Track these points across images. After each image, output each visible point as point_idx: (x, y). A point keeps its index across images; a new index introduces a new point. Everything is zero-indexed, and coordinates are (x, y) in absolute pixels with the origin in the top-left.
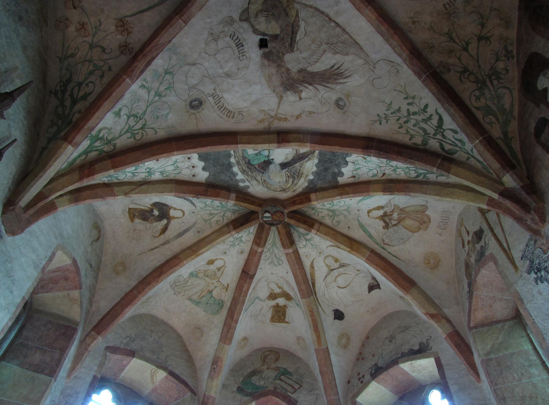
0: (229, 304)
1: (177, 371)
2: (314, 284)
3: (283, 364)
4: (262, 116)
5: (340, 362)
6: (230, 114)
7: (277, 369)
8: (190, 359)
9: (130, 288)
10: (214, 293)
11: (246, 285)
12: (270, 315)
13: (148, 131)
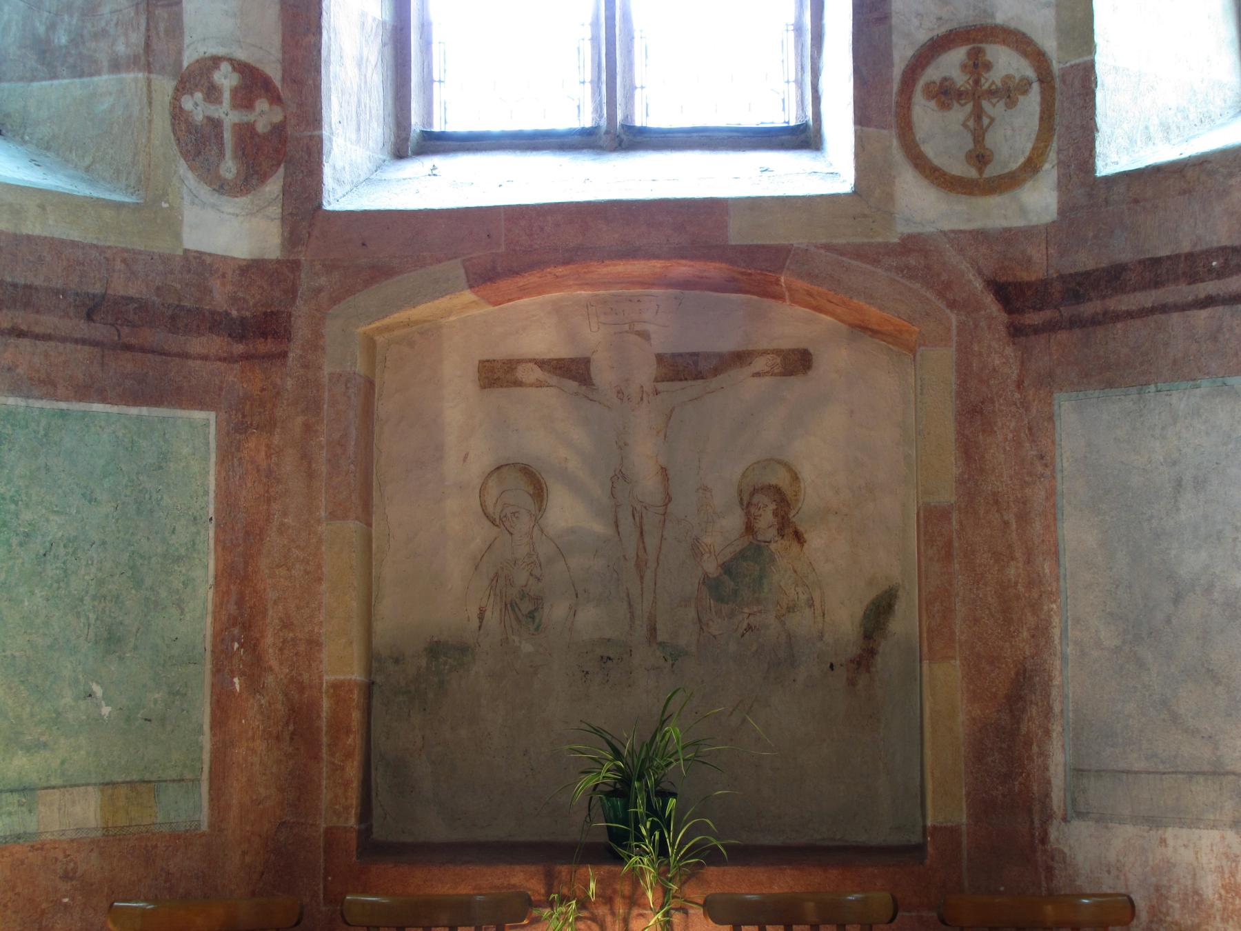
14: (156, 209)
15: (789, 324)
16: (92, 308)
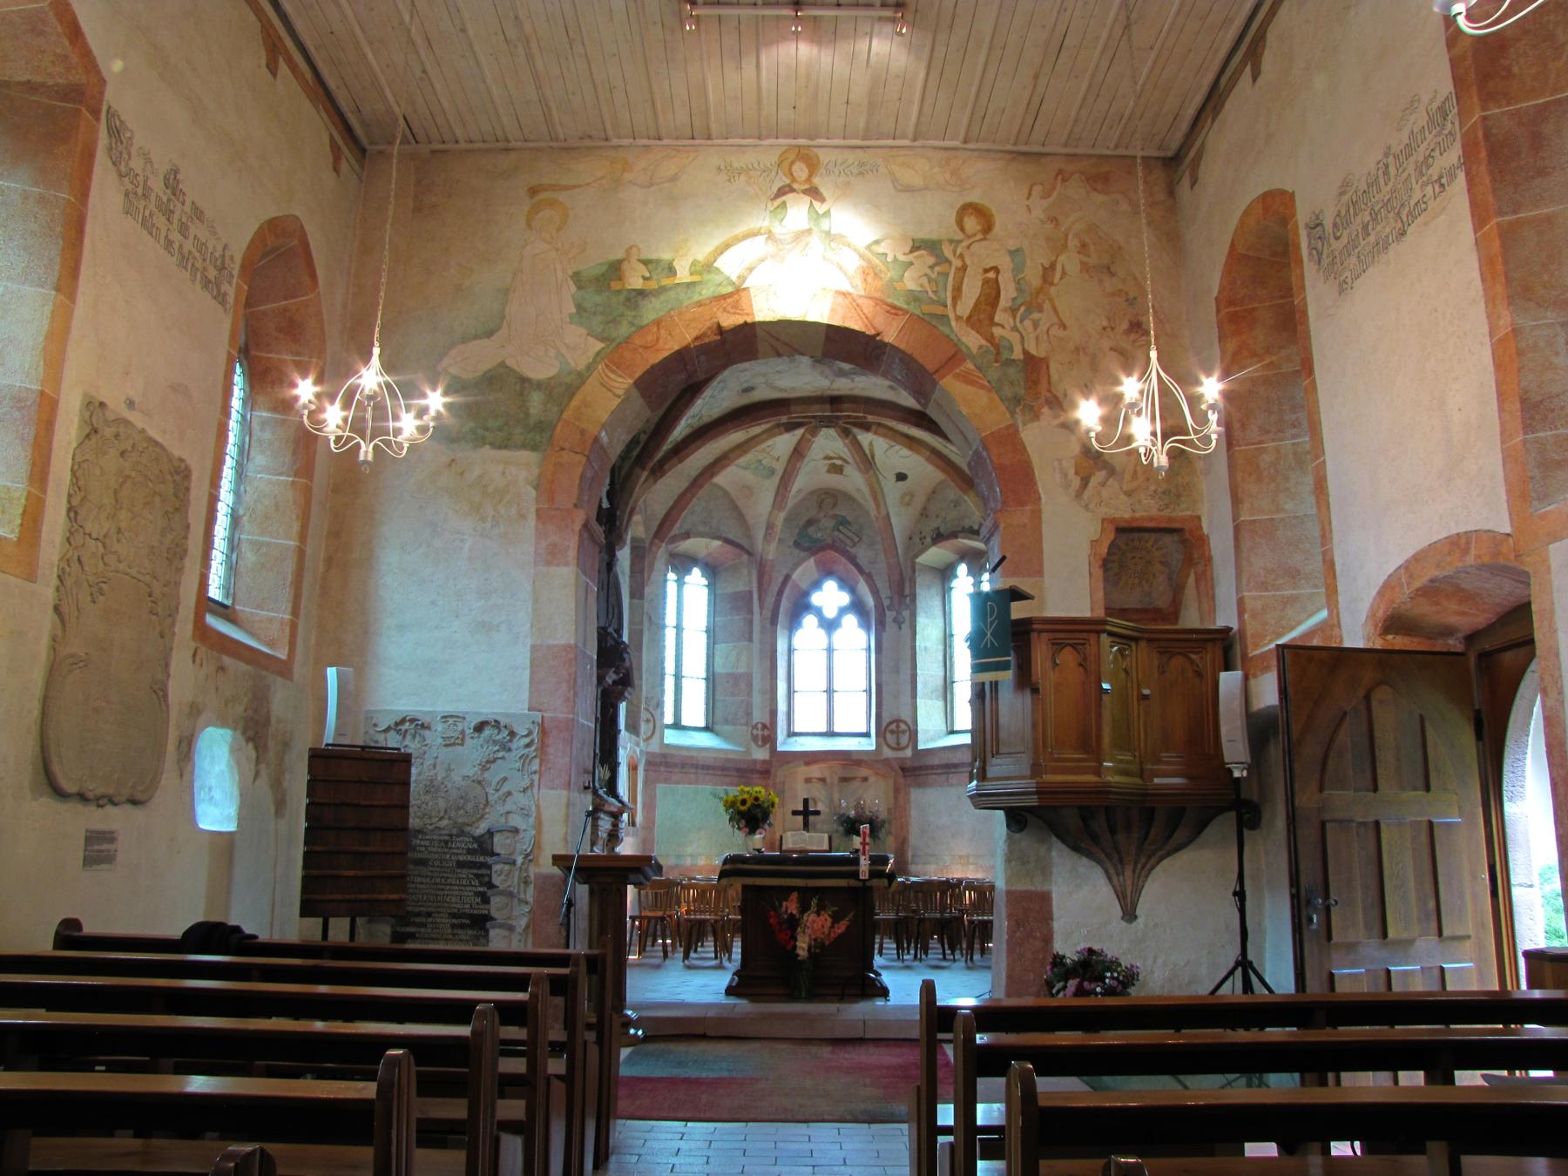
1: (730, 536)
3: (842, 511)
5: (900, 521)
6: (781, 390)
7: (835, 516)
8: (740, 517)
14: (748, 751)
15: (864, 772)
16: (738, 770)
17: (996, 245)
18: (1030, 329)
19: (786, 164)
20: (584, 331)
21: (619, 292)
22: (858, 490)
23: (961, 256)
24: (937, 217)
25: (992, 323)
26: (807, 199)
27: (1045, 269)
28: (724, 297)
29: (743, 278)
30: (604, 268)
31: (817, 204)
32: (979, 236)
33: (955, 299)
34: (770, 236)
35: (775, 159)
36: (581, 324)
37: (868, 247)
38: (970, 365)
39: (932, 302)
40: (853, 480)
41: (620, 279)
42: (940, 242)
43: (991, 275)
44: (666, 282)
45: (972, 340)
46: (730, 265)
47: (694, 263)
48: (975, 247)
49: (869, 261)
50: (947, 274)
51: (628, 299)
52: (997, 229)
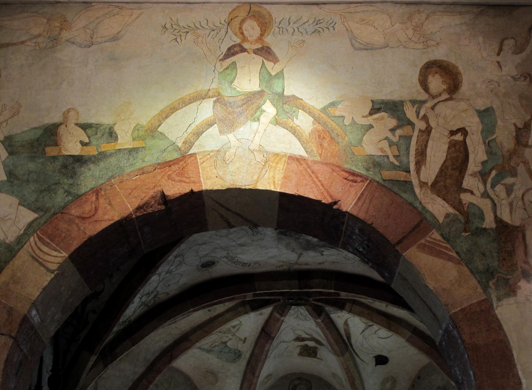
0: (248, 355)
2: (349, 338)
4: (281, 263)
6: (244, 264)
9: (138, 376)
10: (229, 344)
11: (268, 345)
12: (298, 350)
13: (160, 296)
17: (463, 105)
18: (503, 195)
19: (236, 23)
20: (14, 200)
21: (54, 158)
22: (334, 375)
23: (425, 118)
24: (400, 79)
25: (461, 190)
26: (259, 59)
27: (518, 130)
28: (169, 164)
29: (189, 144)
30: (39, 132)
31: (269, 65)
32: (445, 96)
33: (419, 164)
34: (219, 99)
35: (224, 17)
36: (12, 193)
37: (324, 110)
38: (436, 235)
39: (395, 167)
40: (328, 364)
41: (56, 144)
42: (402, 103)
43: (459, 137)
44: (106, 147)
45: (438, 208)
46: (176, 129)
47: (136, 128)
48: (440, 108)
49: (325, 124)
50: (409, 138)
51: (65, 166)
52: (465, 88)
